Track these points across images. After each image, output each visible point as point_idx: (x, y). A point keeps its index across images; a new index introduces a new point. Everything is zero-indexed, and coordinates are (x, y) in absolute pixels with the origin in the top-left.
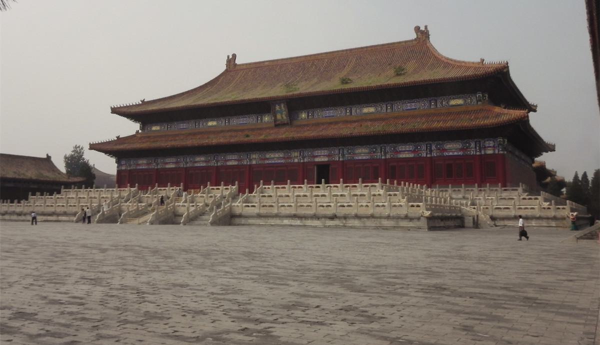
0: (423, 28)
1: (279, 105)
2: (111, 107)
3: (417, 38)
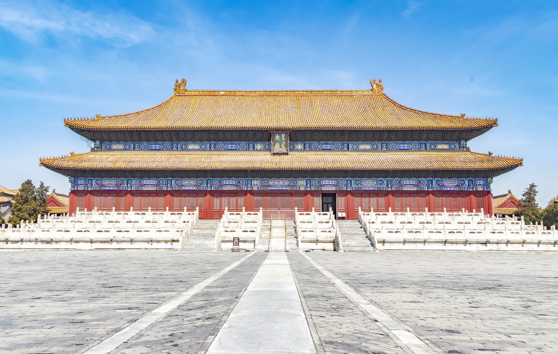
2: (65, 119)
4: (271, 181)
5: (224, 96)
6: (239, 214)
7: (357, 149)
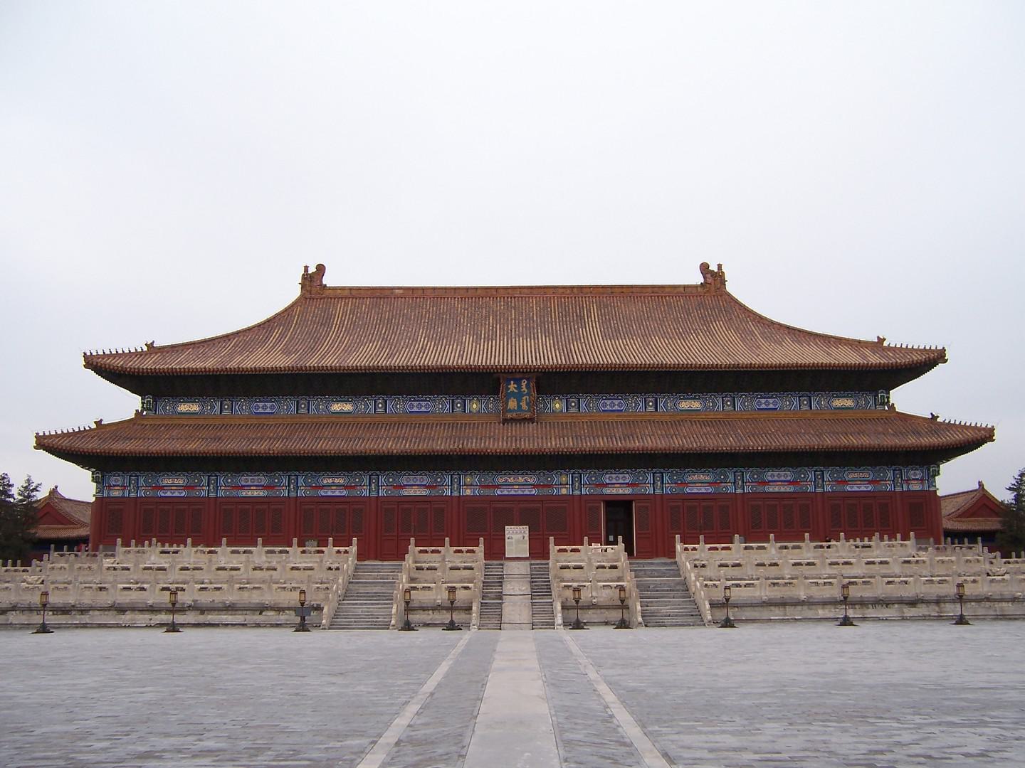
0: (714, 268)
1: (518, 381)
2: (85, 354)
3: (705, 282)
4: (501, 477)
6: (438, 552)
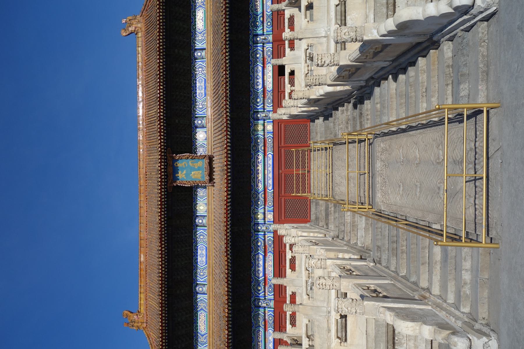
5: (146, 256)
7: (203, 34)
